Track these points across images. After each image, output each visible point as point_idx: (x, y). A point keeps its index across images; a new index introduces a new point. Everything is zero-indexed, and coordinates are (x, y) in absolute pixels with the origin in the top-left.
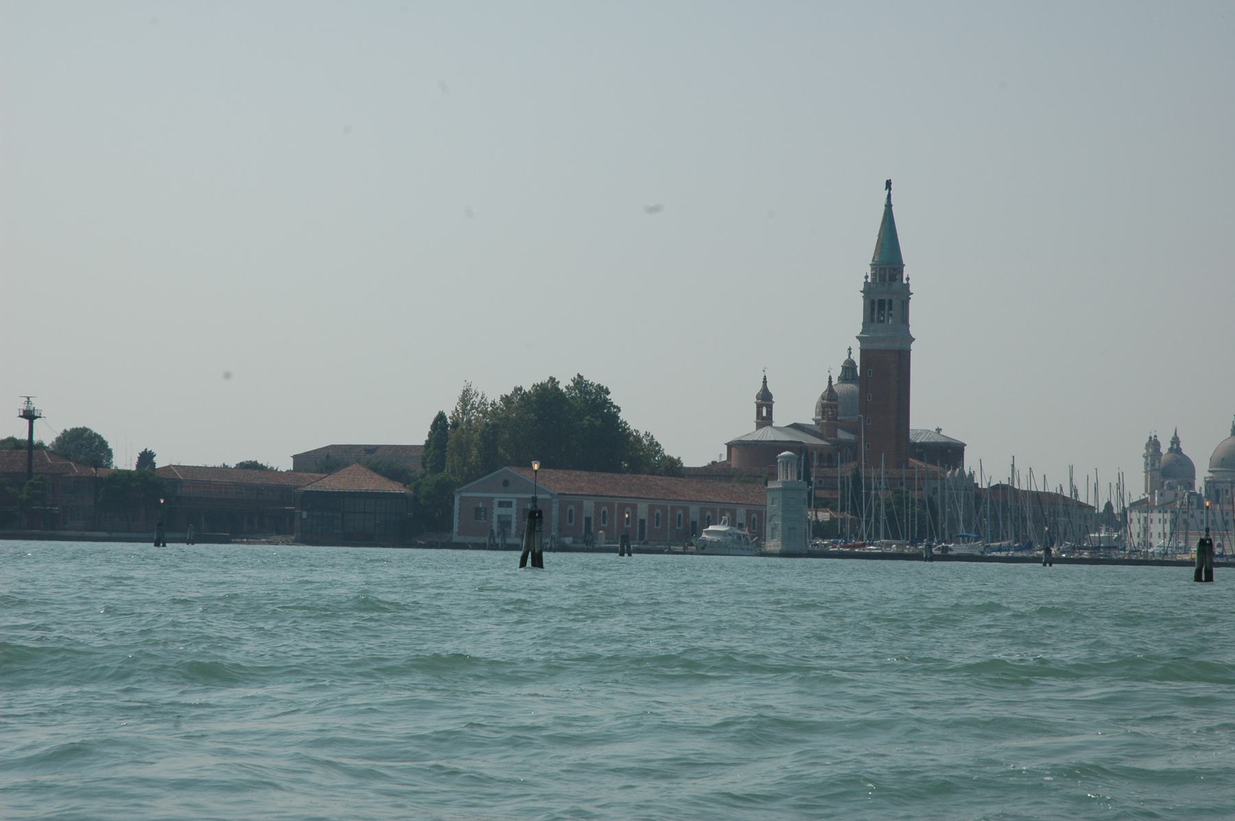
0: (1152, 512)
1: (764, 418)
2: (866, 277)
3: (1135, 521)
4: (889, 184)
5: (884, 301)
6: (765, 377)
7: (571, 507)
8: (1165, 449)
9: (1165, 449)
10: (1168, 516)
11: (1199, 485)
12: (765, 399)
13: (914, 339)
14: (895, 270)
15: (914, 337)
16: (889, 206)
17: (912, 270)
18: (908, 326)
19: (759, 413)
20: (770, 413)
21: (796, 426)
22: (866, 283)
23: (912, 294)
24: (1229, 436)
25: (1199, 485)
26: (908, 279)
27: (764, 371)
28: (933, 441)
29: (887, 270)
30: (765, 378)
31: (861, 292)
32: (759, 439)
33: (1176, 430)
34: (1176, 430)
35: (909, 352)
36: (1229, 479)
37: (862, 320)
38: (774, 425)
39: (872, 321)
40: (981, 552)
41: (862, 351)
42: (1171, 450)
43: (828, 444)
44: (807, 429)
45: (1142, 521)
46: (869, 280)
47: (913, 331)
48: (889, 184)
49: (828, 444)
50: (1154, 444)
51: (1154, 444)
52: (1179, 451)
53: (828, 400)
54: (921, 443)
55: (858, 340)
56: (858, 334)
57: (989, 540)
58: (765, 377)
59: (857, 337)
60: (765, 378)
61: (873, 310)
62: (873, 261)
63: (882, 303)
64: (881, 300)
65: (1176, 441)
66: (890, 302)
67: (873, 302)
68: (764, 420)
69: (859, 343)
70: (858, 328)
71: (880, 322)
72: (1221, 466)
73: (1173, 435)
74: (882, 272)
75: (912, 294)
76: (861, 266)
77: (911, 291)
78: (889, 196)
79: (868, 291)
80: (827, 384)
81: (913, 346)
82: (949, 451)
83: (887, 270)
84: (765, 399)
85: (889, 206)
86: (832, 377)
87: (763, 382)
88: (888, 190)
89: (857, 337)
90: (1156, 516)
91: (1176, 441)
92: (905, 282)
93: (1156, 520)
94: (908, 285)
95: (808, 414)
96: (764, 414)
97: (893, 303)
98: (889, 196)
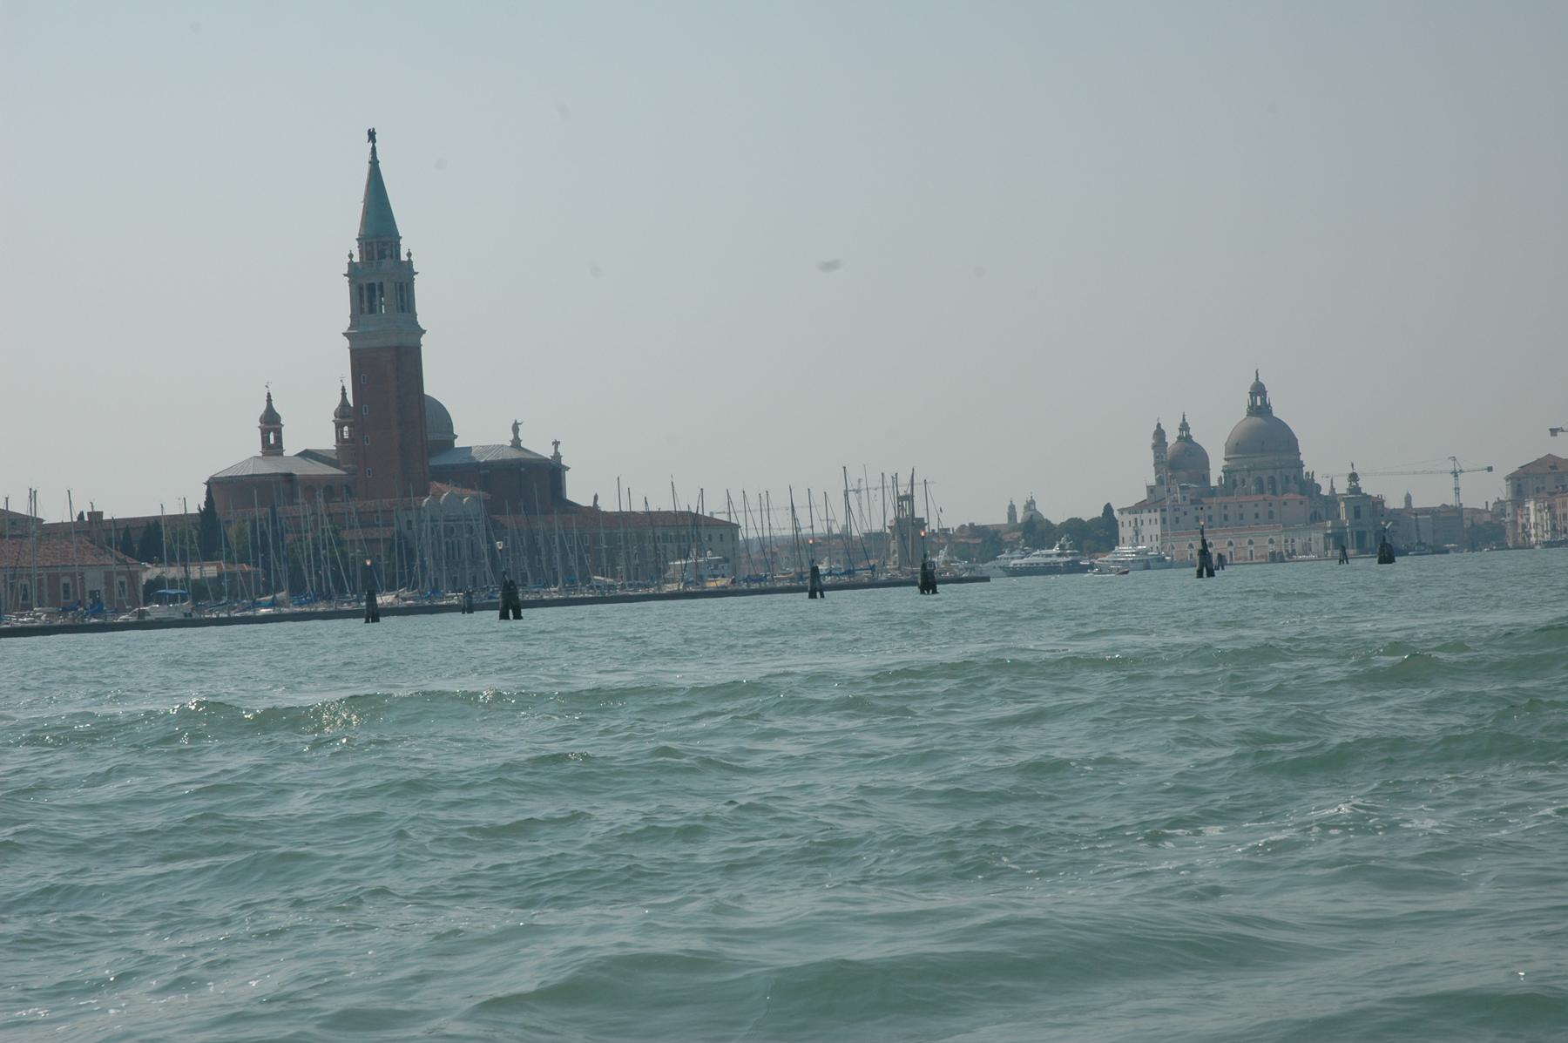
0: (1142, 513)
1: (271, 447)
2: (351, 256)
3: (1126, 523)
4: (372, 135)
5: (373, 284)
6: (269, 394)
7: (66, 580)
8: (1171, 438)
9: (1171, 438)
10: (1157, 515)
11: (1216, 476)
12: (271, 422)
13: (424, 332)
14: (385, 244)
15: (424, 329)
16: (374, 163)
17: (412, 240)
18: (415, 315)
19: (265, 440)
20: (279, 439)
21: (306, 454)
22: (351, 264)
23: (417, 273)
24: (1245, 417)
25: (1216, 476)
26: (409, 254)
27: (267, 387)
28: (500, 458)
29: (375, 246)
30: (269, 396)
31: (345, 275)
32: (235, 474)
33: (1184, 416)
34: (1184, 416)
35: (418, 348)
36: (1245, 467)
37: (349, 312)
38: (285, 454)
39: (362, 311)
40: (185, 615)
41: (355, 353)
42: (1180, 438)
43: (344, 473)
44: (321, 455)
45: (1133, 524)
46: (356, 259)
47: (422, 321)
48: (372, 135)
49: (344, 473)
50: (1160, 434)
51: (1160, 434)
52: (1188, 439)
53: (340, 417)
54: (486, 462)
55: (345, 338)
56: (345, 330)
57: (141, 600)
58: (269, 394)
59: (344, 334)
60: (269, 396)
61: (362, 301)
62: (359, 235)
63: (371, 287)
64: (370, 284)
65: (1184, 427)
66: (381, 285)
67: (361, 288)
68: (272, 447)
69: (348, 342)
70: (345, 323)
71: (372, 310)
72: (1236, 452)
73: (1181, 421)
74: (369, 248)
75: (417, 273)
76: (345, 240)
77: (415, 270)
78: (374, 150)
79: (354, 272)
80: (341, 396)
81: (423, 340)
82: (523, 469)
83: (375, 246)
84: (271, 422)
85: (374, 163)
86: (346, 388)
87: (267, 401)
88: (371, 144)
89: (344, 334)
90: (1146, 516)
91: (1184, 427)
92: (404, 258)
93: (1146, 523)
94: (410, 262)
95: (325, 439)
96: (272, 442)
97: (385, 287)
98: (374, 150)
